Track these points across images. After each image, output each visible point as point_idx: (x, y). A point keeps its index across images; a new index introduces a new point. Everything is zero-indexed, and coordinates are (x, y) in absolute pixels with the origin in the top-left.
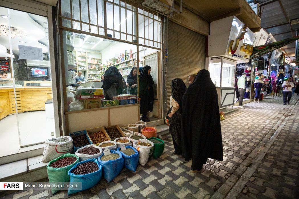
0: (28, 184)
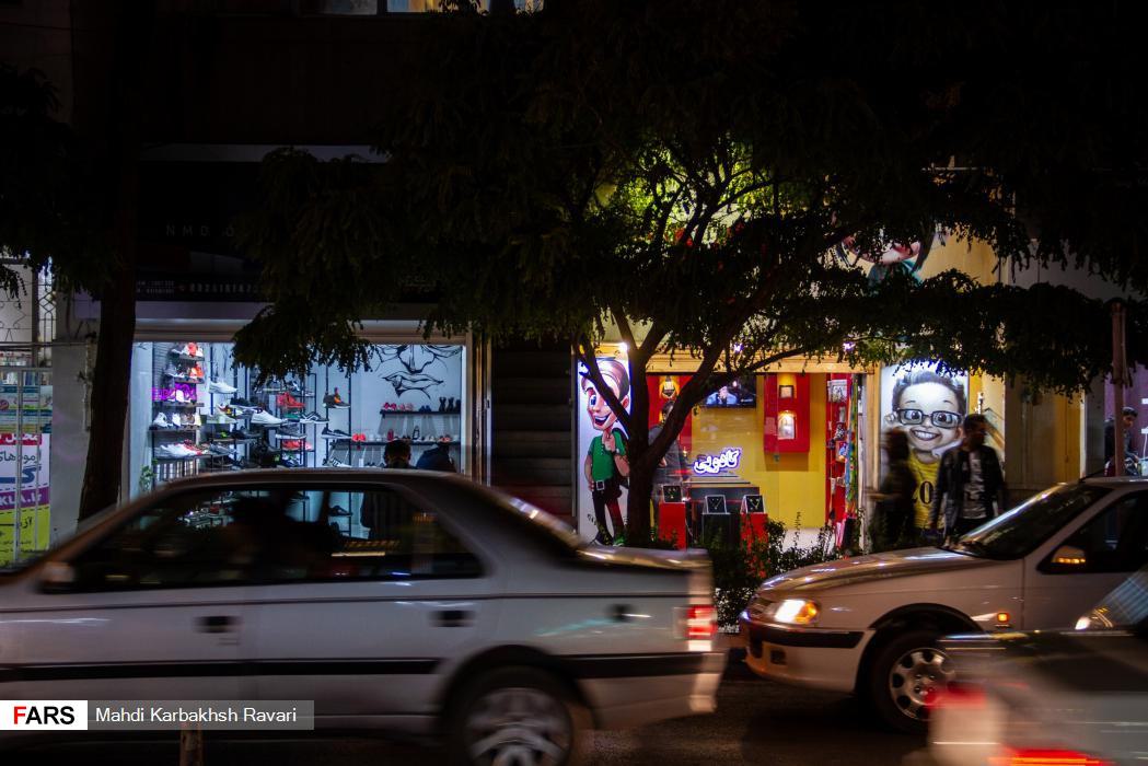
0: (108, 709)
